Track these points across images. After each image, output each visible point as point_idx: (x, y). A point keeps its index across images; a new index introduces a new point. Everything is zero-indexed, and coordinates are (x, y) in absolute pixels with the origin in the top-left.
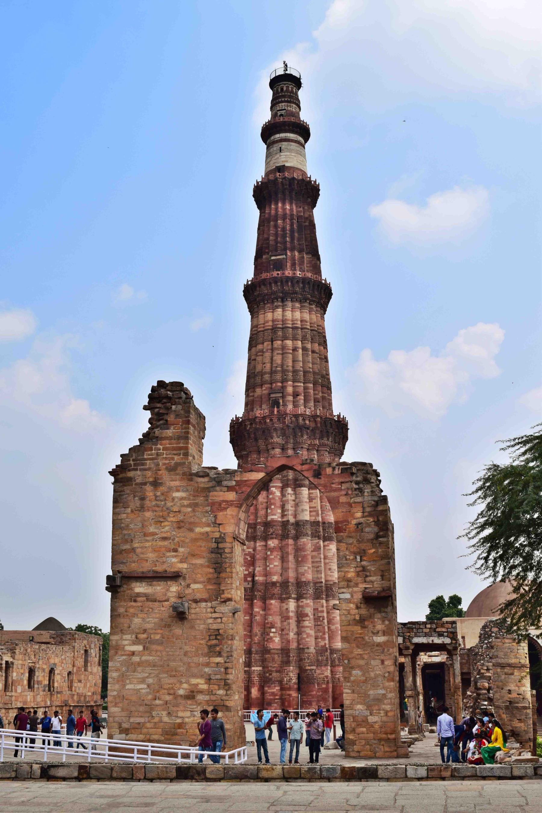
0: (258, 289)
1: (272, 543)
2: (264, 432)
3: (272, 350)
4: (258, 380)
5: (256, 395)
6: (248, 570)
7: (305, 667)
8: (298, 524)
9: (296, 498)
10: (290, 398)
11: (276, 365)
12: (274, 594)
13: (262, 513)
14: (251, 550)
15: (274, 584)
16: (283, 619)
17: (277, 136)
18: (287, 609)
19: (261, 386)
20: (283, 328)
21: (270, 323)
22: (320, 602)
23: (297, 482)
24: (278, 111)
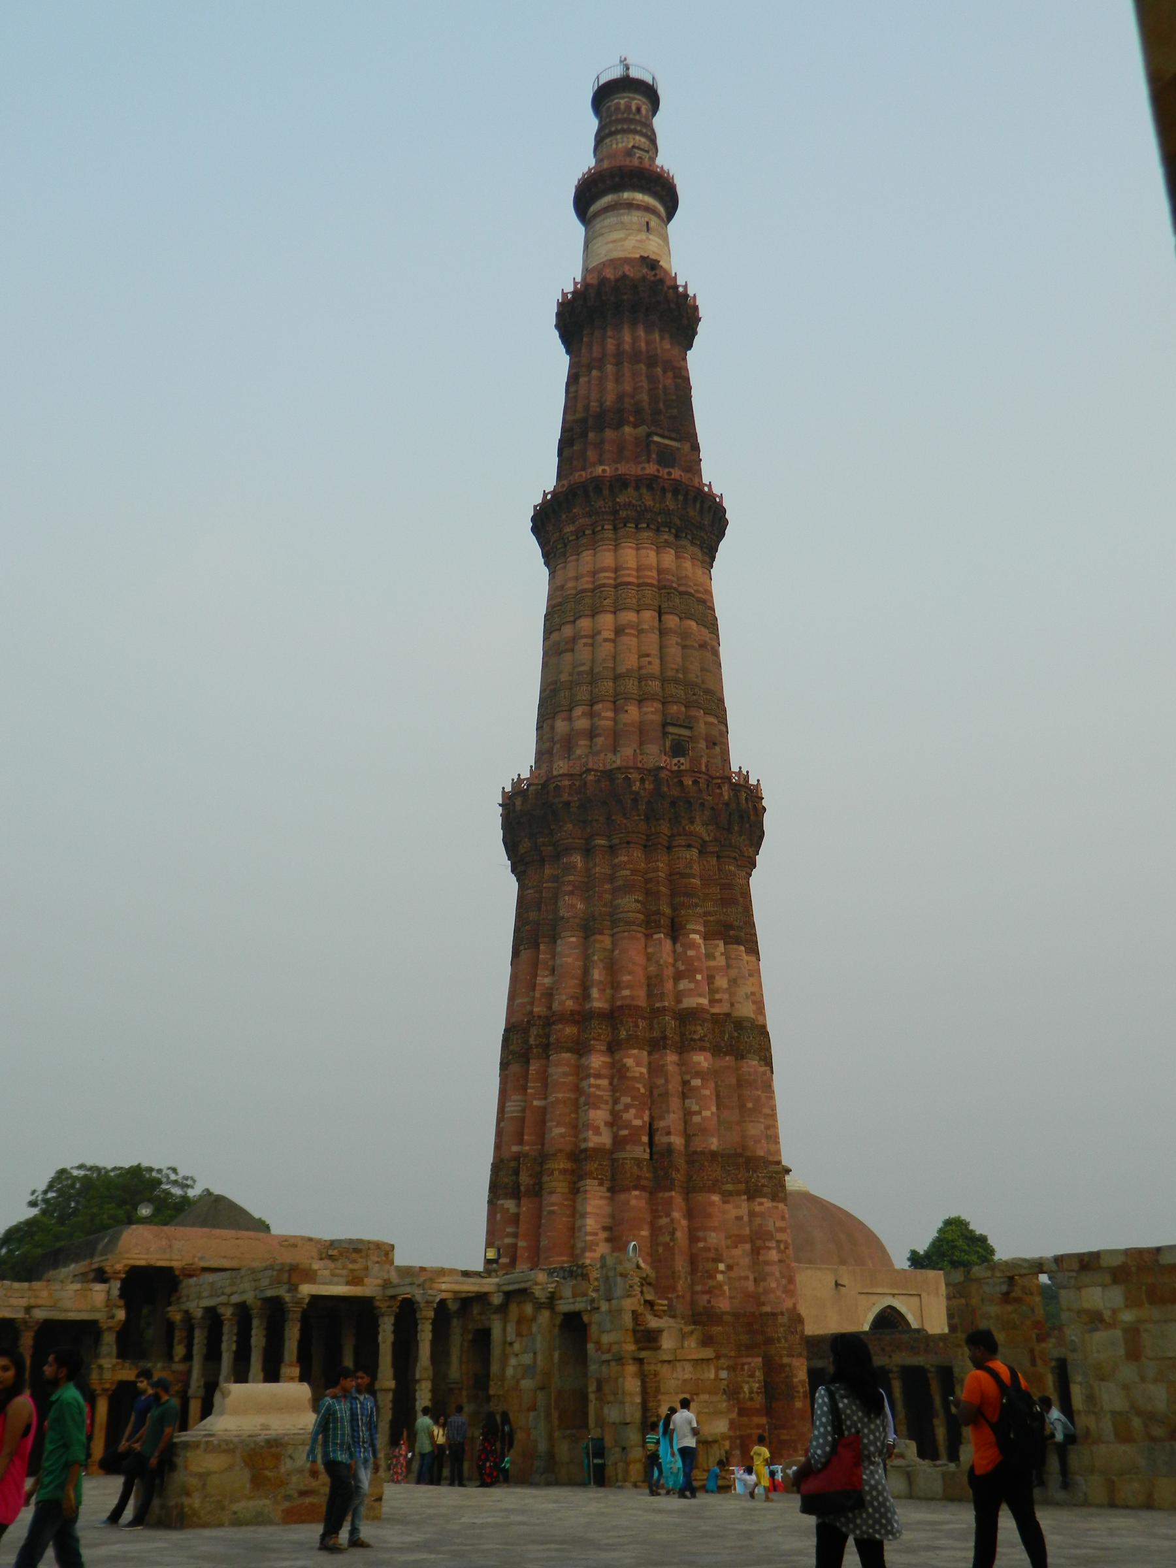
0: (630, 490)
1: (702, 1060)
2: (673, 804)
3: (662, 632)
4: (631, 686)
5: (624, 718)
6: (642, 1118)
7: (781, 1357)
8: (739, 1024)
9: (728, 966)
10: (702, 745)
11: (675, 666)
12: (717, 1181)
13: (669, 985)
14: (644, 1070)
15: (714, 1155)
16: (729, 1242)
17: (639, 197)
18: (739, 1218)
19: (640, 702)
20: (681, 593)
21: (654, 574)
22: (777, 1208)
23: (732, 933)
24: (634, 147)
